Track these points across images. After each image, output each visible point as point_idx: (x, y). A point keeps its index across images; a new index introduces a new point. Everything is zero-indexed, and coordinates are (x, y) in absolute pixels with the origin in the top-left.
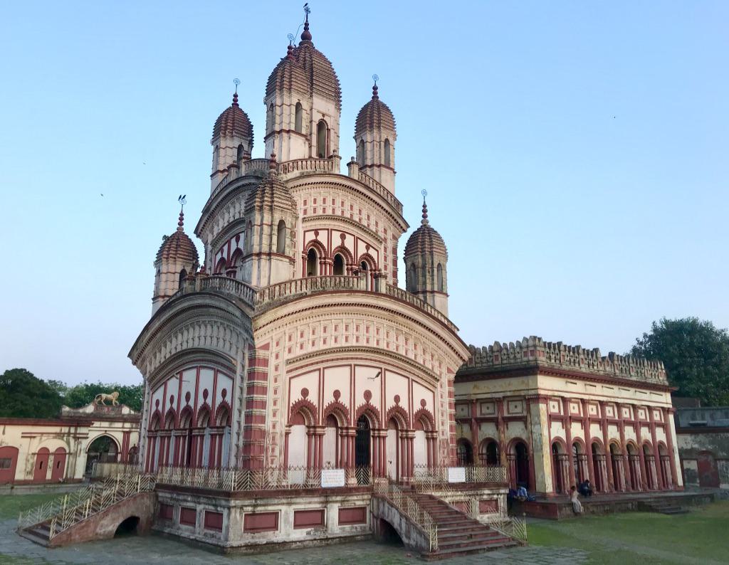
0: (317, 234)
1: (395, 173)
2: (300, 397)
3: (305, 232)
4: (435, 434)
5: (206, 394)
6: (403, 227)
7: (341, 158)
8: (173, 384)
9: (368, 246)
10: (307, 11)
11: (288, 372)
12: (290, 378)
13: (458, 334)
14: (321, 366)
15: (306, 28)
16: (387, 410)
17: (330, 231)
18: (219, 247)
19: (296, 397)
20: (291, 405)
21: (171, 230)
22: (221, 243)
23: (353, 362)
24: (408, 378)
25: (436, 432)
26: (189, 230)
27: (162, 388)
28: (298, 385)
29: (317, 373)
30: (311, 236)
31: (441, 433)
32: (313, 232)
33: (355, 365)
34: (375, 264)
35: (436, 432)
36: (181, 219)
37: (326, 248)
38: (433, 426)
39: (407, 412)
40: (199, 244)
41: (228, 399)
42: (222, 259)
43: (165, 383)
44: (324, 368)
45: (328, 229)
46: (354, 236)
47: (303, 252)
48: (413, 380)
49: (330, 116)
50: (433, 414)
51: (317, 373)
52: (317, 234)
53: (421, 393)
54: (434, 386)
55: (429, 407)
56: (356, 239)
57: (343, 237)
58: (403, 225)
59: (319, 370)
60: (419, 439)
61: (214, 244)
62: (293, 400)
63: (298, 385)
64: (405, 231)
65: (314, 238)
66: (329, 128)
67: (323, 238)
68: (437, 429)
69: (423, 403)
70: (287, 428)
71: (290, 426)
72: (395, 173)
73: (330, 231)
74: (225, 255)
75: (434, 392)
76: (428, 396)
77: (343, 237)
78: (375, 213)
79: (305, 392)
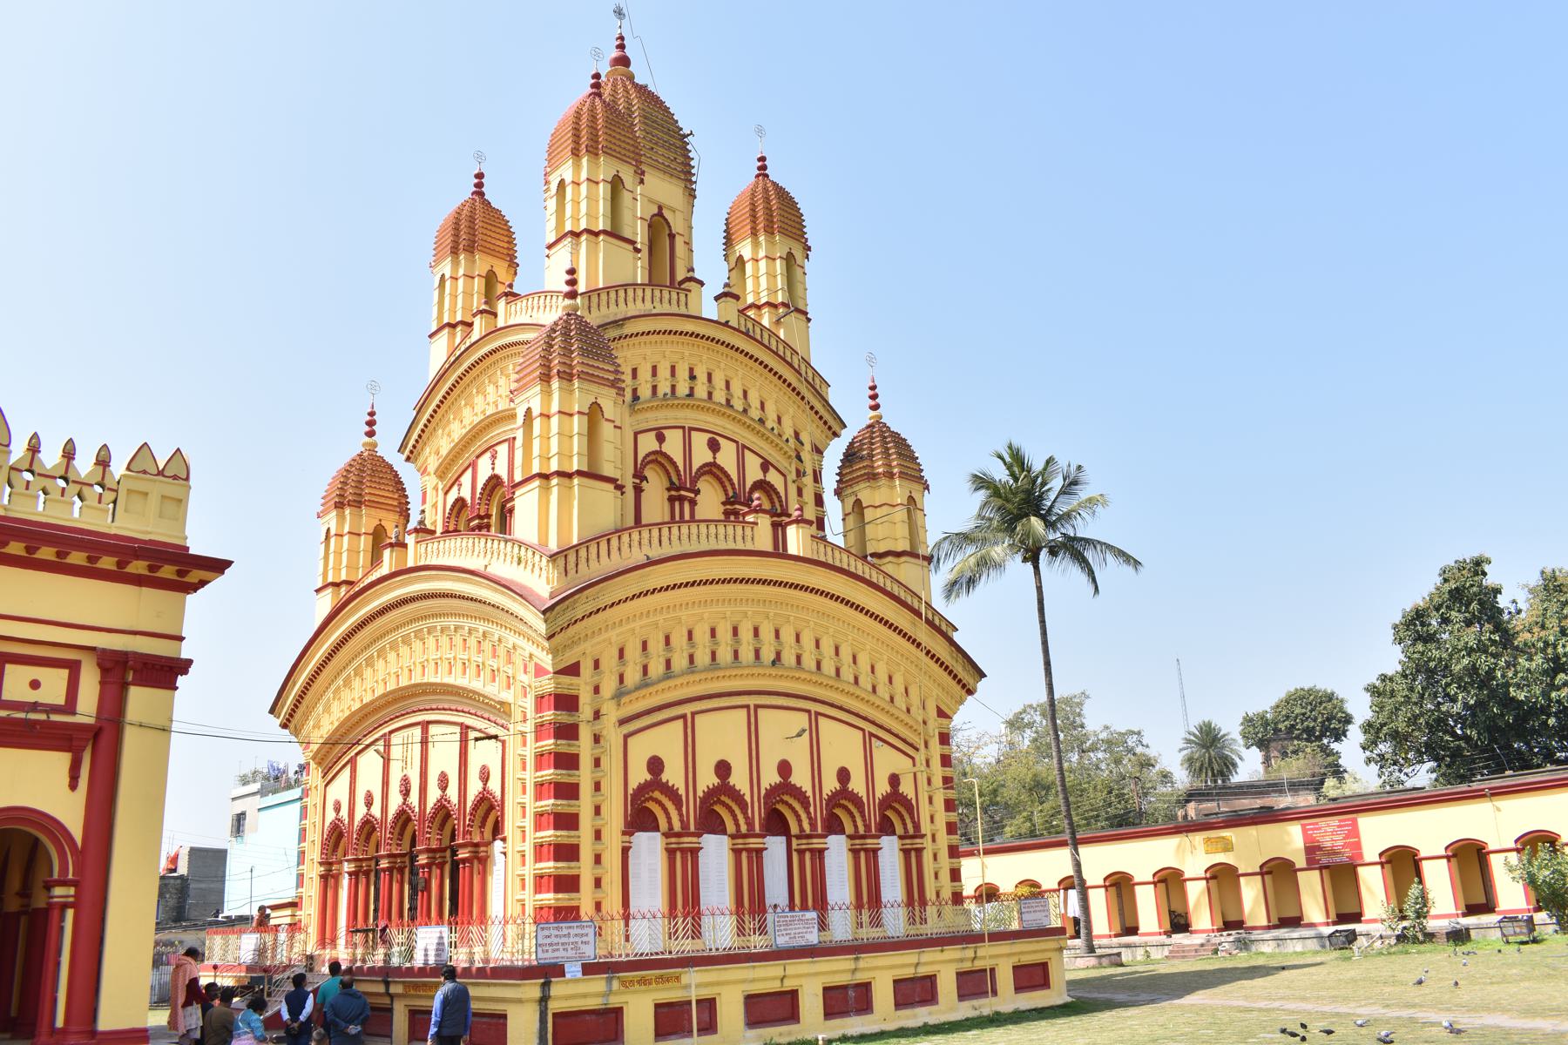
0: (661, 438)
1: (809, 320)
3: (636, 434)
5: (443, 781)
6: (832, 424)
7: (702, 283)
8: (369, 764)
9: (766, 466)
10: (619, 13)
11: (622, 722)
12: (626, 737)
13: (956, 637)
14: (687, 709)
15: (621, 47)
16: (825, 796)
17: (687, 432)
18: (451, 475)
19: (639, 775)
20: (630, 791)
21: (352, 445)
22: (456, 469)
23: (752, 701)
25: (923, 836)
26: (388, 449)
27: (346, 774)
29: (680, 723)
30: (648, 444)
31: (929, 837)
32: (654, 433)
33: (757, 707)
34: (780, 501)
35: (923, 836)
36: (371, 423)
37: (681, 468)
38: (917, 826)
39: (865, 800)
40: (407, 472)
41: (494, 785)
42: (460, 503)
43: (353, 762)
44: (693, 714)
45: (683, 428)
46: (736, 442)
47: (635, 476)
50: (914, 802)
51: (680, 723)
52: (661, 438)
53: (888, 761)
54: (911, 745)
55: (906, 788)
56: (742, 449)
57: (714, 446)
58: (831, 422)
59: (684, 717)
60: (890, 850)
61: (441, 473)
62: (633, 784)
63: (642, 748)
64: (836, 435)
65: (655, 446)
67: (673, 446)
68: (923, 832)
70: (626, 838)
71: (631, 834)
72: (809, 320)
73: (687, 432)
74: (466, 493)
75: (913, 758)
76: (899, 764)
77: (714, 446)
79: (655, 765)
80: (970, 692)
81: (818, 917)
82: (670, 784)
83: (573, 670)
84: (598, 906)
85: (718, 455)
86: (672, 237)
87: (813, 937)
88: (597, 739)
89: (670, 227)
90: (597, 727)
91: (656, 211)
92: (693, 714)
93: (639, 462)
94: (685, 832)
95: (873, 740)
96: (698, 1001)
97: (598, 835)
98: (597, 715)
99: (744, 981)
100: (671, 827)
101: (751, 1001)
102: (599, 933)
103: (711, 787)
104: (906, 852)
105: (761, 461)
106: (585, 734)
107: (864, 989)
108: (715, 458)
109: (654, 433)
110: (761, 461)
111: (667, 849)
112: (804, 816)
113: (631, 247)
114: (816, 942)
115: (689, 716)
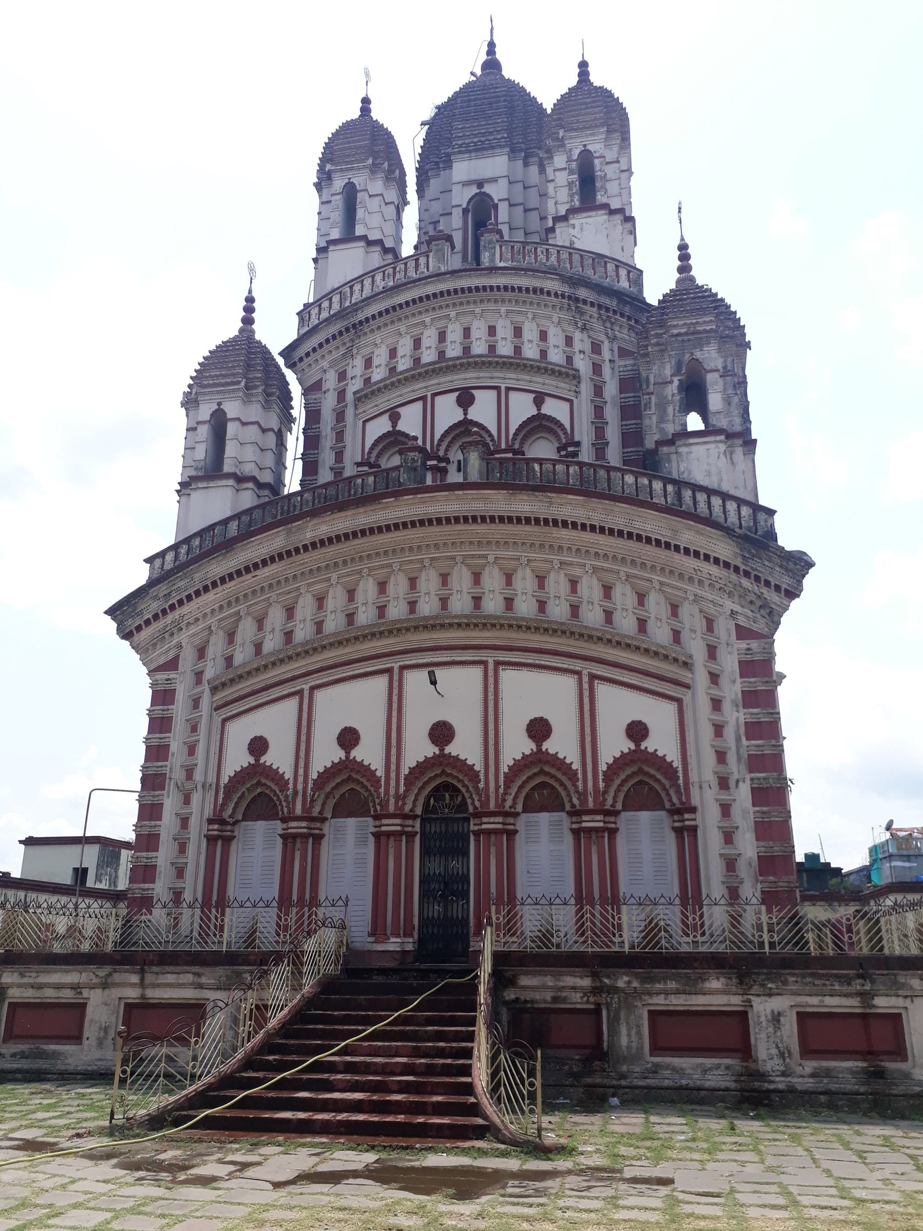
0: (395, 418)
4: (687, 816)
9: (539, 399)
24: (578, 673)
29: (293, 703)
30: (382, 426)
33: (403, 668)
45: (423, 398)
48: (593, 677)
49: (494, 180)
56: (502, 395)
59: (300, 693)
66: (496, 202)
68: (695, 801)
69: (637, 731)
73: (427, 402)
75: (679, 701)
78: (556, 319)
79: (258, 746)
80: (793, 593)
82: (274, 767)
83: (172, 665)
85: (471, 410)
86: (496, 207)
89: (492, 199)
91: (474, 190)
93: (367, 450)
104: (679, 832)
105: (532, 396)
108: (466, 414)
109: (386, 416)
110: (532, 396)
113: (362, 244)
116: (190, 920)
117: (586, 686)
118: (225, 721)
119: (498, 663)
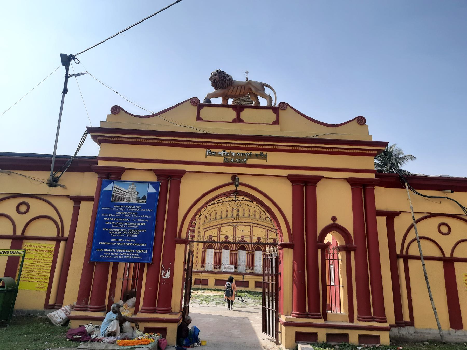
2: (240, 239)
10: (247, 72)
11: (204, 229)
12: (205, 232)
14: (219, 226)
28: (208, 234)
48: (268, 230)
63: (208, 234)
79: (211, 237)
81: (235, 267)
84: (197, 261)
87: (233, 270)
88: (199, 232)
90: (199, 230)
92: (220, 227)
94: (217, 249)
95: (269, 231)
96: (202, 279)
97: (198, 249)
98: (199, 228)
99: (214, 277)
100: (215, 248)
101: (216, 281)
102: (196, 266)
103: (223, 241)
106: (196, 231)
107: (257, 283)
111: (230, 253)
112: (248, 247)
114: (233, 271)
115: (219, 228)
116: (199, 266)
117: (267, 231)
118: (205, 232)
119: (253, 226)
